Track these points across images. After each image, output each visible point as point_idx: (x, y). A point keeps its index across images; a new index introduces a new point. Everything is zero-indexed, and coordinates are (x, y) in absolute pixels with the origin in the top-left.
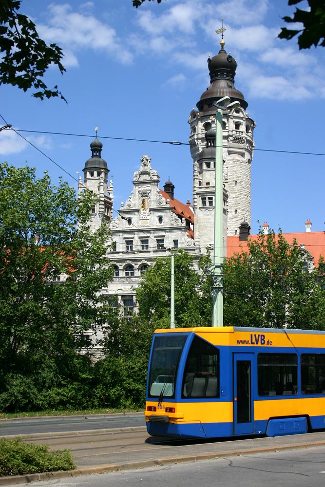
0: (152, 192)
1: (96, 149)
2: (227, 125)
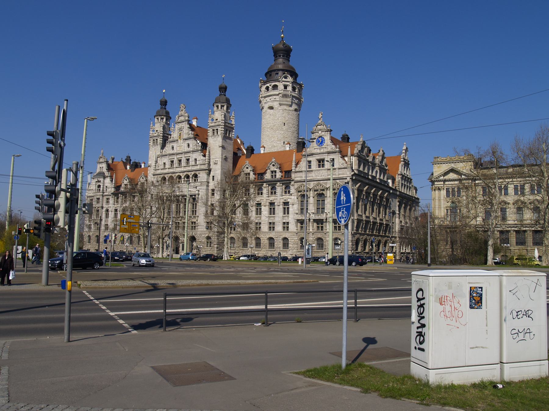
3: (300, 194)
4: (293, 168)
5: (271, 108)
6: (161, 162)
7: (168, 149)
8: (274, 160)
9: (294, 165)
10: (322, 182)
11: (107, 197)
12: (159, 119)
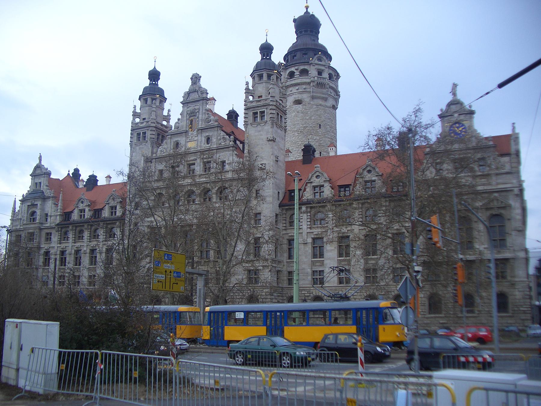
0: (201, 111)
1: (154, 75)
11: (48, 231)
12: (149, 100)
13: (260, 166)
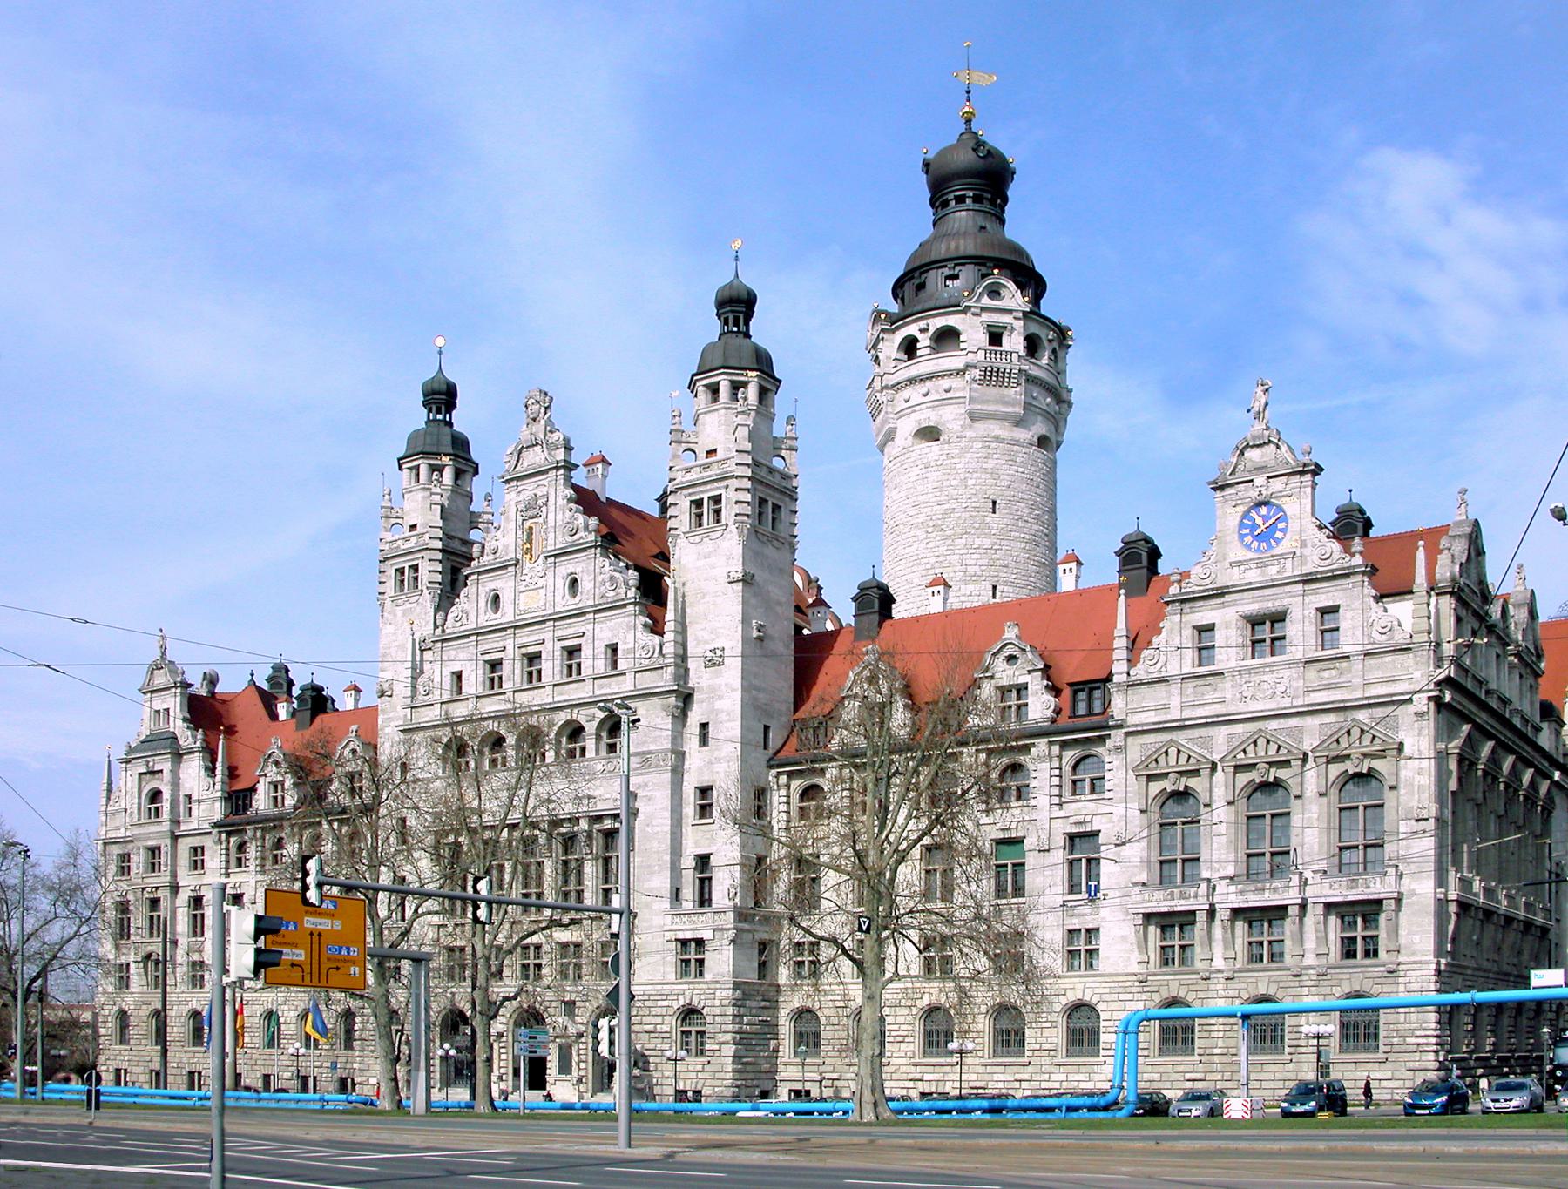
2: (962, 338)
3: (1155, 787)
4: (1119, 668)
5: (929, 434)
6: (438, 673)
7: (471, 607)
8: (1011, 633)
9: (1120, 654)
10: (1273, 725)
13: (709, 654)
